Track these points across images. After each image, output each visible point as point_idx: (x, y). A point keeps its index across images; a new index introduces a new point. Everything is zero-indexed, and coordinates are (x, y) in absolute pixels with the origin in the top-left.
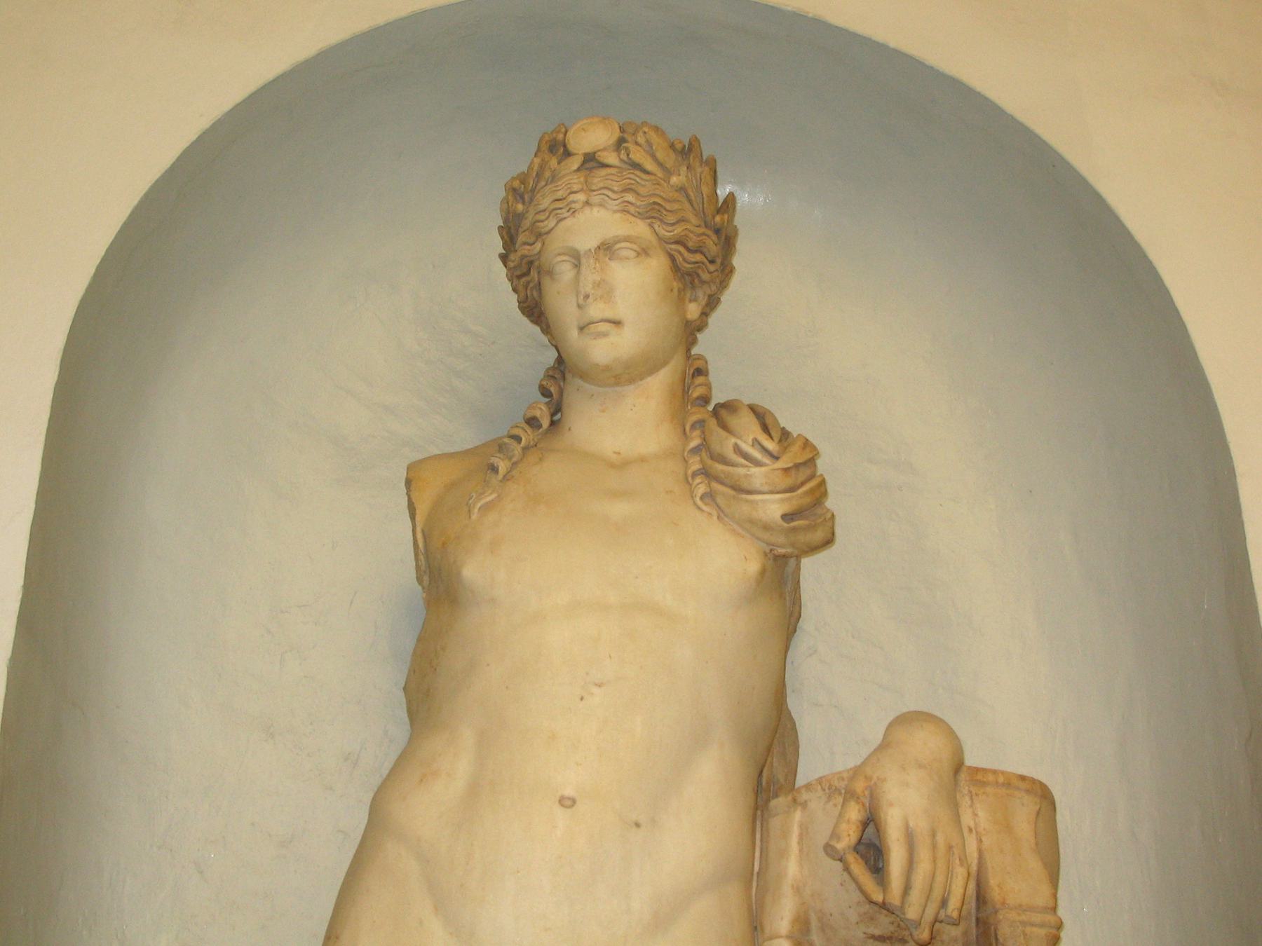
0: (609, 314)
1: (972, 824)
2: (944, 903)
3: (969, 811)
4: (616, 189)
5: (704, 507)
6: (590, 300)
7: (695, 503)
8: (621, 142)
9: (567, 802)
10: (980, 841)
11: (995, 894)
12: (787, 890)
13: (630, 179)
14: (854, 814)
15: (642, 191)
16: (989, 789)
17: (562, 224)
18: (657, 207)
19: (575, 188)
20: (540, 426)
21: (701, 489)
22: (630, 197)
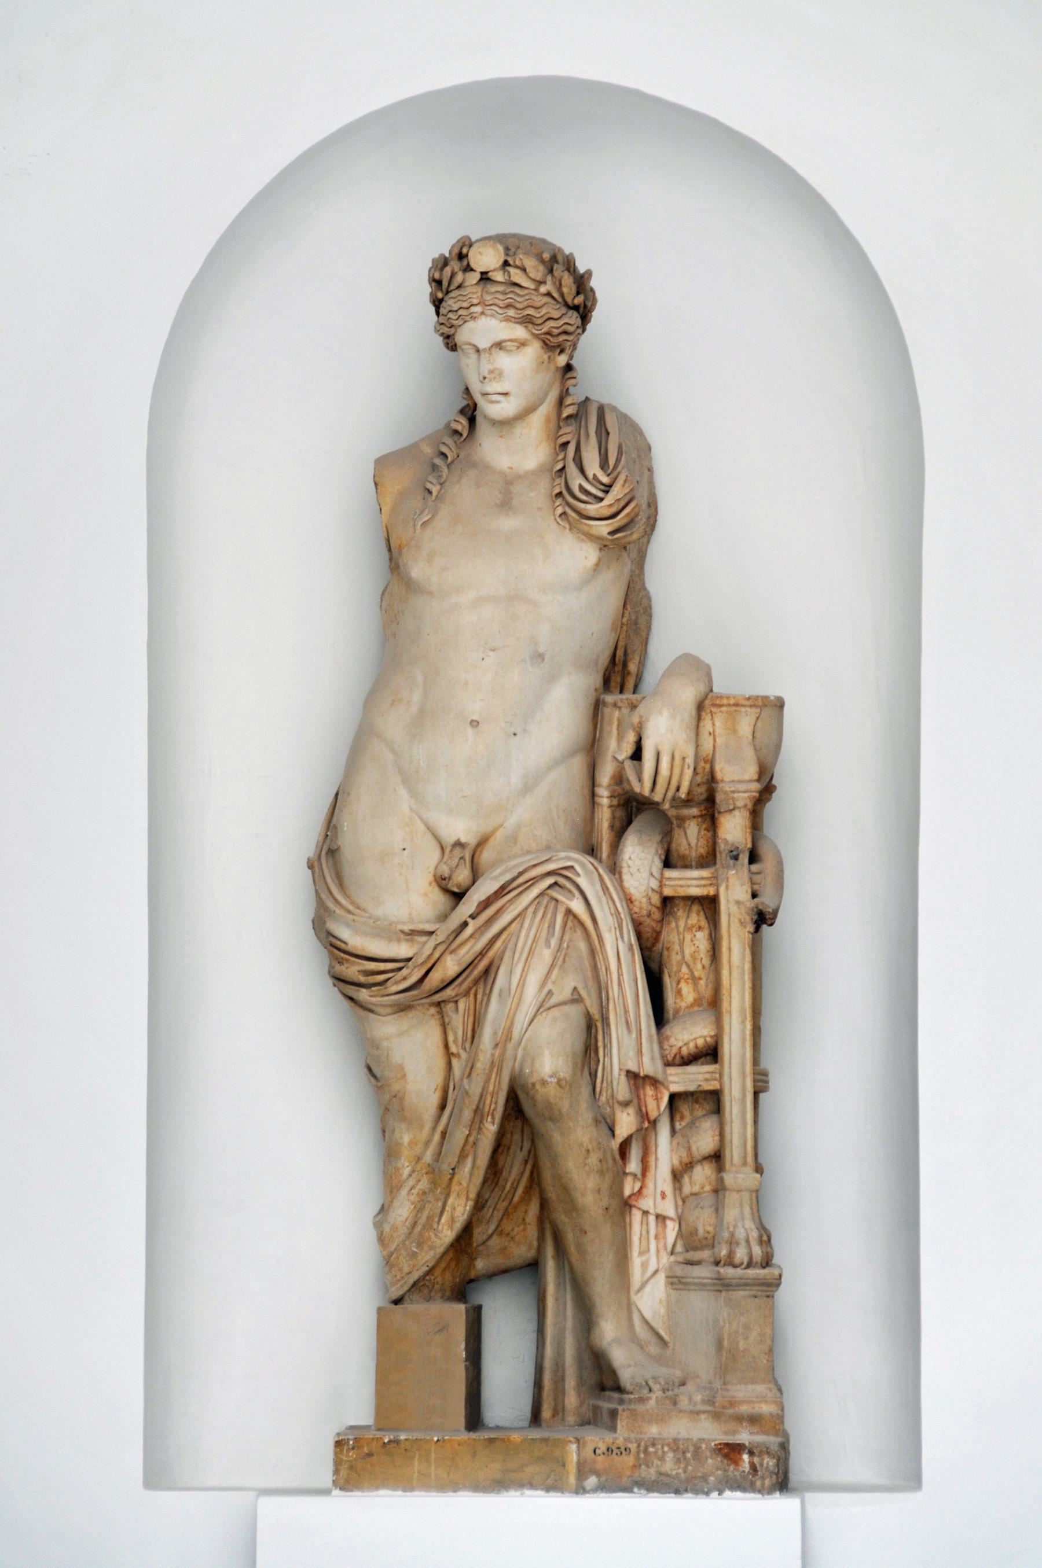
0: (500, 390)
1: (711, 731)
2: (678, 789)
3: (710, 722)
4: (501, 306)
5: (561, 523)
6: (486, 380)
7: (555, 519)
8: (506, 263)
9: (474, 724)
10: (715, 740)
11: (719, 775)
12: (609, 758)
13: (511, 298)
14: (631, 737)
15: (518, 305)
16: (724, 709)
17: (467, 324)
18: (529, 317)
19: (475, 301)
20: (461, 435)
21: (560, 510)
22: (511, 312)
